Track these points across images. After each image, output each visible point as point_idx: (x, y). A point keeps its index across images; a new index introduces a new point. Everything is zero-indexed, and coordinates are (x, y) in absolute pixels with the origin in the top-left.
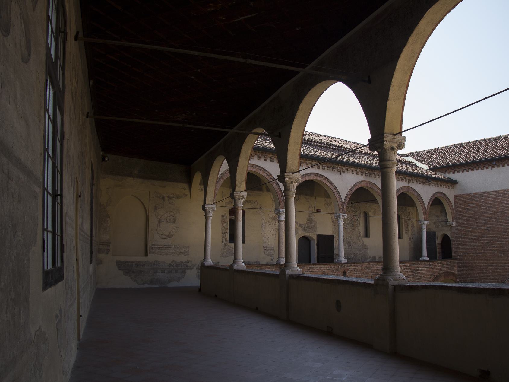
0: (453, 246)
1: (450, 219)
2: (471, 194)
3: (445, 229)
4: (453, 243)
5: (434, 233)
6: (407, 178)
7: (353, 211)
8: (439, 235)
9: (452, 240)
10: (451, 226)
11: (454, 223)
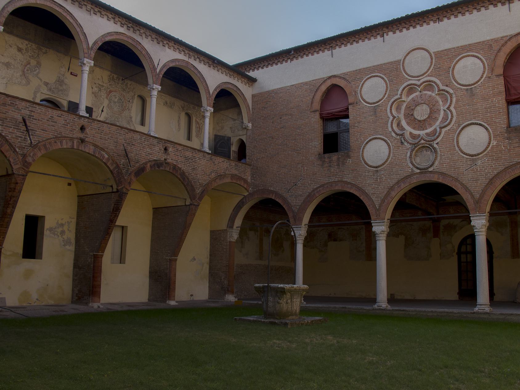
0: (247, 151)
1: (245, 121)
2: (268, 92)
3: (241, 133)
4: (247, 148)
5: (229, 139)
6: (186, 52)
7: (124, 90)
8: (235, 141)
9: (247, 145)
10: (246, 128)
11: (250, 125)
